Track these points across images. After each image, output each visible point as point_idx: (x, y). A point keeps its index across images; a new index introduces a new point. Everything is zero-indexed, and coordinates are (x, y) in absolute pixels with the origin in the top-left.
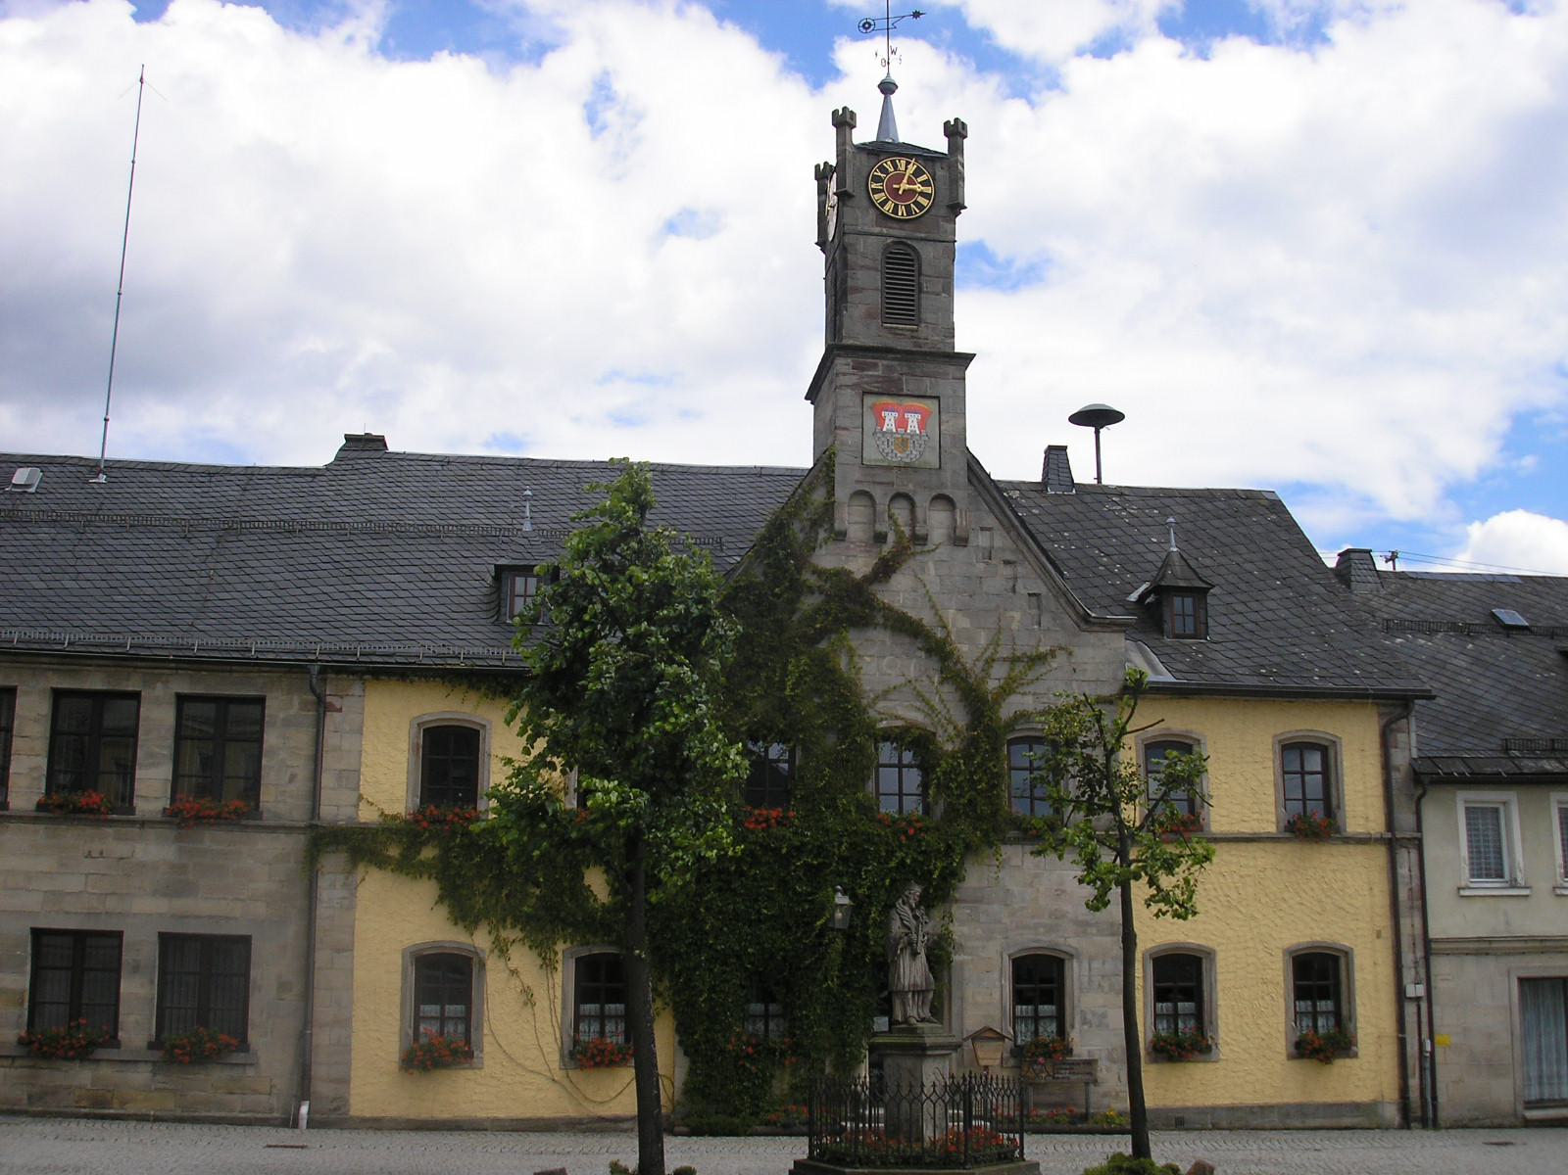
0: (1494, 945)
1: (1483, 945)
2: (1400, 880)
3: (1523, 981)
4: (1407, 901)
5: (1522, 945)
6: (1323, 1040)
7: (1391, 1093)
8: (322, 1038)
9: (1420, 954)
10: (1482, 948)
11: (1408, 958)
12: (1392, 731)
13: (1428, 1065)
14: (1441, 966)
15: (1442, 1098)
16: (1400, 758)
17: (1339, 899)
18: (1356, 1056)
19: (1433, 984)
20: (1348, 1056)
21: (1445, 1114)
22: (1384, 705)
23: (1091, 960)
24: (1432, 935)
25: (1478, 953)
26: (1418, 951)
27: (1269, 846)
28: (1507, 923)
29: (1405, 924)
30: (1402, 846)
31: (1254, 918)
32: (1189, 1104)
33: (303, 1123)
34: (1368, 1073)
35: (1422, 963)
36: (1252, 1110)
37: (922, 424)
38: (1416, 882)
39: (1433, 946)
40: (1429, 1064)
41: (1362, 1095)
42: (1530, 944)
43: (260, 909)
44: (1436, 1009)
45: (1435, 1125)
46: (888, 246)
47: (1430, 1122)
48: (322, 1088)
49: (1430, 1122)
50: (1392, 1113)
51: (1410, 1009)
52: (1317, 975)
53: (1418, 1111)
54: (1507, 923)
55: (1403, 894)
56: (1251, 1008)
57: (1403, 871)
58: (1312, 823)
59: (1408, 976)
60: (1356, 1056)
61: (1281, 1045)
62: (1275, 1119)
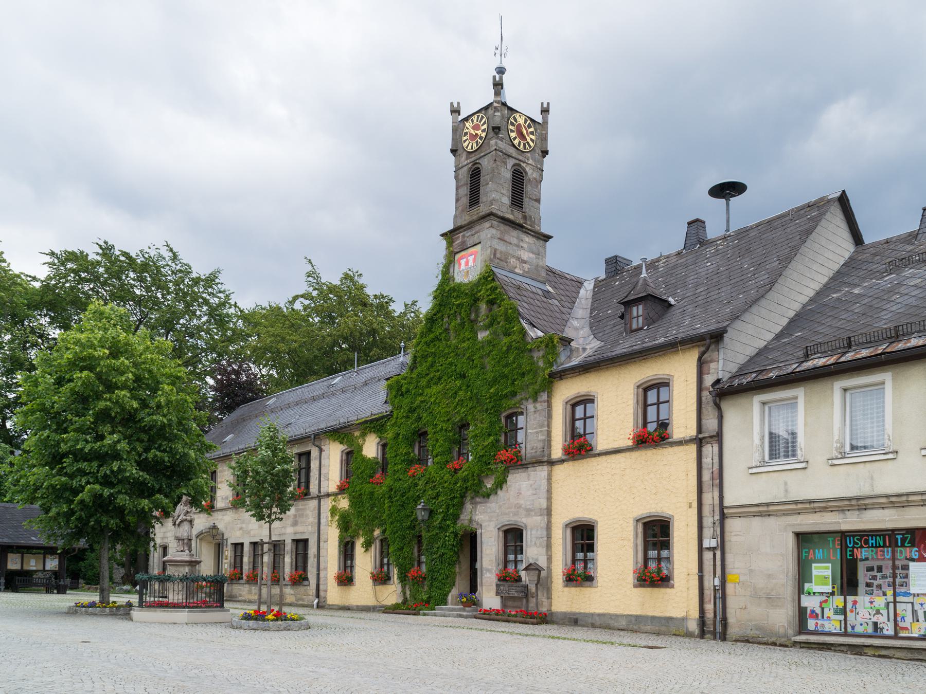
0: (771, 508)
1: (761, 509)
2: (704, 466)
3: (798, 535)
4: (710, 480)
5: (793, 507)
6: (653, 577)
7: (695, 614)
8: (322, 574)
9: (717, 517)
10: (763, 510)
11: (708, 521)
12: (707, 362)
13: (719, 594)
14: (733, 525)
15: (731, 620)
16: (709, 380)
17: (665, 483)
18: (673, 587)
19: (727, 538)
20: (667, 587)
21: (733, 631)
23: (531, 529)
24: (727, 503)
25: (761, 515)
26: (718, 517)
27: (628, 454)
28: (786, 491)
29: (708, 498)
30: (708, 443)
32: (582, 611)
34: (680, 600)
35: (717, 523)
36: (611, 616)
37: (474, 261)
38: (716, 467)
39: (726, 511)
40: (721, 593)
42: (800, 506)
43: (310, 528)
44: (729, 558)
45: (723, 637)
47: (718, 636)
48: (322, 593)
49: (718, 636)
50: (693, 626)
51: (708, 556)
52: (656, 532)
53: (713, 627)
54: (786, 491)
55: (706, 476)
56: (617, 553)
57: (707, 461)
58: (652, 436)
59: (707, 532)
60: (673, 587)
61: (631, 578)
62: (623, 623)
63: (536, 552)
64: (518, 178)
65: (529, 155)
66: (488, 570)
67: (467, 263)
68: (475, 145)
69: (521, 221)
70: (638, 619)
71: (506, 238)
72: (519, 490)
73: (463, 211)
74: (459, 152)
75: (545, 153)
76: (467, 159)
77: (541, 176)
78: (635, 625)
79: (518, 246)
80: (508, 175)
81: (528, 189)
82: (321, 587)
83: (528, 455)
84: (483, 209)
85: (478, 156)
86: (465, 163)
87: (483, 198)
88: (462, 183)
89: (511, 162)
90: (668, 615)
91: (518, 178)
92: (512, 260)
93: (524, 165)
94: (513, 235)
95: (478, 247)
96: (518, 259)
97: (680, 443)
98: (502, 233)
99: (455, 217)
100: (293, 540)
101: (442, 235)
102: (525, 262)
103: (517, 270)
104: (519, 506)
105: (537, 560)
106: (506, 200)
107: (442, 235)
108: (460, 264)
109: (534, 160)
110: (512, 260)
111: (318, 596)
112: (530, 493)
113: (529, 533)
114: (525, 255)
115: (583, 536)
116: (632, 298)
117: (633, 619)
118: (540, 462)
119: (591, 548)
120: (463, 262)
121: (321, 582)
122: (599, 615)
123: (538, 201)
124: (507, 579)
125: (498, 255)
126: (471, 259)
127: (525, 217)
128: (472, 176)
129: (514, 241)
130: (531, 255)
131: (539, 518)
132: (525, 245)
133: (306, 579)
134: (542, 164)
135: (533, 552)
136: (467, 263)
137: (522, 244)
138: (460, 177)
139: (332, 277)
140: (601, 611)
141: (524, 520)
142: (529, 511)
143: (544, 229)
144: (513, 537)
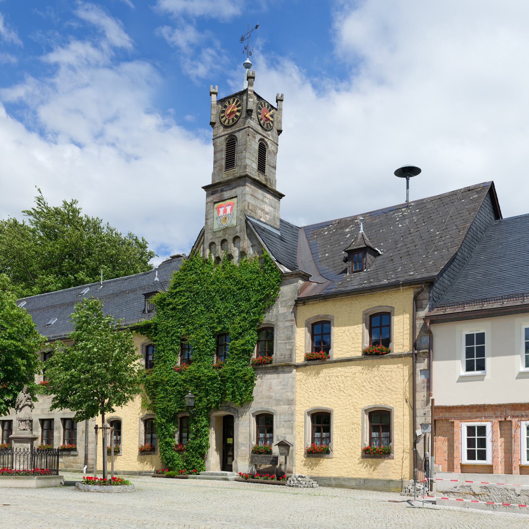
6: (377, 450)
17: (389, 385)
18: (393, 458)
22: (417, 288)
23: (280, 415)
31: (350, 395)
32: (321, 475)
33: (85, 472)
36: (344, 479)
37: (231, 210)
41: (396, 477)
46: (227, 139)
48: (90, 461)
52: (380, 420)
56: (349, 434)
60: (393, 458)
62: (354, 483)
63: (284, 432)
64: (262, 148)
65: (269, 132)
66: (243, 445)
67: (225, 211)
68: (231, 121)
69: (264, 182)
70: (365, 480)
71: (256, 195)
72: (271, 385)
73: (220, 170)
74: (216, 126)
75: (280, 132)
76: (224, 131)
77: (277, 149)
78: (364, 485)
79: (263, 201)
80: (256, 147)
81: (268, 158)
82: (89, 457)
83: (278, 360)
84: (237, 172)
85: (234, 130)
86: (223, 134)
87: (238, 162)
88: (220, 148)
89: (258, 137)
90: (389, 478)
91: (262, 148)
92: (259, 212)
93: (266, 140)
94: (260, 193)
95: (235, 200)
96: (263, 210)
97: (400, 356)
98: (253, 190)
99: (214, 175)
100: (62, 419)
101: (203, 188)
102: (267, 213)
103: (262, 219)
104: (270, 398)
105: (285, 437)
106: (255, 166)
107: (203, 188)
108: (219, 212)
109: (273, 137)
110: (259, 212)
111: (86, 463)
112: (279, 387)
113: (278, 417)
114: (268, 208)
115: (321, 421)
116: (354, 248)
117: (362, 481)
118: (289, 366)
119: (328, 429)
120: (222, 210)
121: (90, 452)
122: (335, 479)
123: (275, 168)
124: (260, 452)
125: (250, 208)
126: (228, 208)
127: (266, 180)
128: (228, 145)
129: (260, 197)
130: (271, 209)
131: (287, 406)
132: (267, 201)
133: (75, 449)
134: (278, 140)
135: (280, 432)
136: (225, 211)
137: (265, 200)
138: (218, 144)
139: (55, 202)
140: (336, 476)
141: (274, 408)
142: (278, 402)
143: (279, 189)
144: (265, 422)
